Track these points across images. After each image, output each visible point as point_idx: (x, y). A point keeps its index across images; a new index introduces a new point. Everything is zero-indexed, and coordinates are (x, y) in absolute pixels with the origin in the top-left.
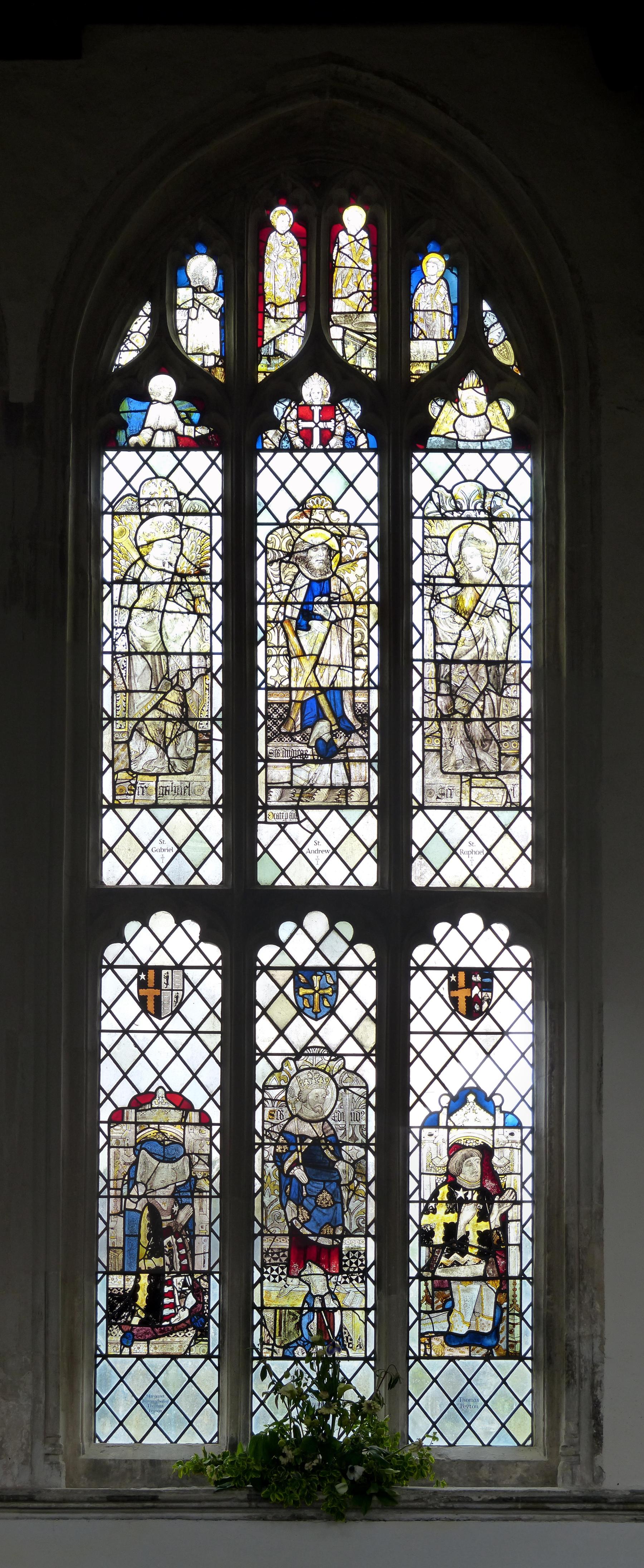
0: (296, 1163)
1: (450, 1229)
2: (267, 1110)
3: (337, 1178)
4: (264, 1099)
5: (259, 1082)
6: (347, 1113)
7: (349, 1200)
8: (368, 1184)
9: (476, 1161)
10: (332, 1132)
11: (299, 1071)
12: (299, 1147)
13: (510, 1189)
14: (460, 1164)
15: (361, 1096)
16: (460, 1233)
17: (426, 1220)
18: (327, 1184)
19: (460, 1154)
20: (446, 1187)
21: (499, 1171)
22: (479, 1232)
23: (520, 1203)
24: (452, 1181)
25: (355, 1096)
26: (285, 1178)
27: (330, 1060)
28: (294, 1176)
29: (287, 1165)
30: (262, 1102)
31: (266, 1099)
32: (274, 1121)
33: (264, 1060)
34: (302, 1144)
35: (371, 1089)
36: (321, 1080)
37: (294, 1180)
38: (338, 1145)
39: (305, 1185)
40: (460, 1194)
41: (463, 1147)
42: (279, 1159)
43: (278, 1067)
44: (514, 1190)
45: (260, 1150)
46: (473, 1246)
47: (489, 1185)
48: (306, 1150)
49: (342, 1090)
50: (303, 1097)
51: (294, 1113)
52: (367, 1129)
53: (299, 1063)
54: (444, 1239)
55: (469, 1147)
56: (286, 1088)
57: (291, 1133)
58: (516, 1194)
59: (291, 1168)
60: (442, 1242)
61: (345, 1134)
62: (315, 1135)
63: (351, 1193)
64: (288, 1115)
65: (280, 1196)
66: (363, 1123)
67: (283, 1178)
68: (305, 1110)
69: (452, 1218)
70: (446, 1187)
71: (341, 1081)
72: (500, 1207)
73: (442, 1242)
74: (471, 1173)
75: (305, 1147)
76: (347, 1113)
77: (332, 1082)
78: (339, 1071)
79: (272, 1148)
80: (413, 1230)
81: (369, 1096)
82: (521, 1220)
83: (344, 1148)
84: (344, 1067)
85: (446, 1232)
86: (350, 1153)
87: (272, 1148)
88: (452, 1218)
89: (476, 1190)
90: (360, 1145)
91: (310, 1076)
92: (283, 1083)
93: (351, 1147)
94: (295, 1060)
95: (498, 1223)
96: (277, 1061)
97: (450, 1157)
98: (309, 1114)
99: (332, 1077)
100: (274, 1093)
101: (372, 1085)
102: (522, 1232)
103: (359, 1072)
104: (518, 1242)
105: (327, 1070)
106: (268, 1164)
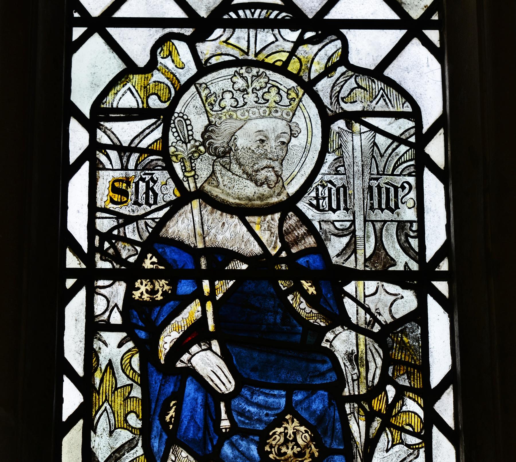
0: (196, 334)
2: (105, 180)
3: (332, 377)
4: (95, 147)
5: (83, 98)
6: (358, 186)
7: (371, 444)
8: (430, 396)
10: (311, 241)
11: (204, 68)
12: (206, 284)
15: (398, 140)
18: (298, 397)
25: (382, 141)
26: (163, 379)
27: (300, 42)
28: (191, 372)
29: (168, 339)
30: (90, 154)
31: (103, 148)
32: (125, 210)
33: (96, 40)
34: (216, 273)
35: (429, 118)
36: (273, 96)
37: (190, 388)
38: (333, 279)
39: (228, 398)
42: (141, 322)
43: (141, 59)
45: (82, 295)
48: (228, 293)
49: (341, 124)
50: (219, 142)
51: (190, 186)
52: (421, 234)
53: (205, 49)
56: (165, 117)
57: (178, 244)
59: (181, 346)
61: (351, 248)
62: (257, 249)
63: (376, 424)
64: (169, 192)
65: (145, 432)
66: (409, 214)
67: (156, 379)
68: (224, 178)
71: (336, 97)
75: (223, 287)
76: (358, 186)
77: (307, 100)
78: (328, 71)
79: (121, 288)
81: (424, 138)
83: (350, 288)
84: (344, 60)
86: (370, 302)
87: (121, 288)
90: (403, 279)
91: (240, 83)
92: (154, 103)
93: (371, 286)
94: (191, 43)
96: (138, 43)
98: (238, 188)
99: (309, 87)
100: (125, 131)
101: (432, 109)
103: (390, 72)
105: (293, 67)
106: (105, 335)
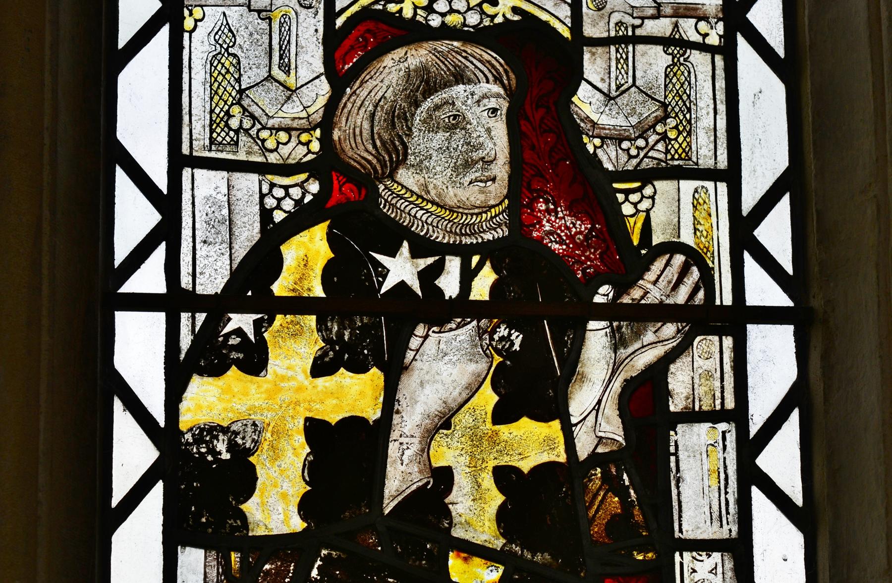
1: (344, 454)
9: (483, 106)
13: (672, 248)
14: (397, 119)
16: (400, 477)
17: (209, 400)
19: (391, 72)
20: (320, 231)
21: (610, 158)
22: (505, 476)
23: (735, 320)
24: (351, 201)
40: (401, 269)
41: (413, 32)
44: (695, 257)
46: (470, 550)
47: (558, 226)
54: (305, 507)
55: (446, 32)
58: (707, 280)
60: (297, 524)
69: (354, 394)
70: (320, 231)
72: (618, 342)
73: (297, 524)
74: (459, 166)
80: (132, 453)
82: (739, 415)
85: (314, 470)
88: (354, 394)
89: (489, 251)
95: (613, 428)
97: (340, 76)
102: (750, 476)
104: (729, 529)
